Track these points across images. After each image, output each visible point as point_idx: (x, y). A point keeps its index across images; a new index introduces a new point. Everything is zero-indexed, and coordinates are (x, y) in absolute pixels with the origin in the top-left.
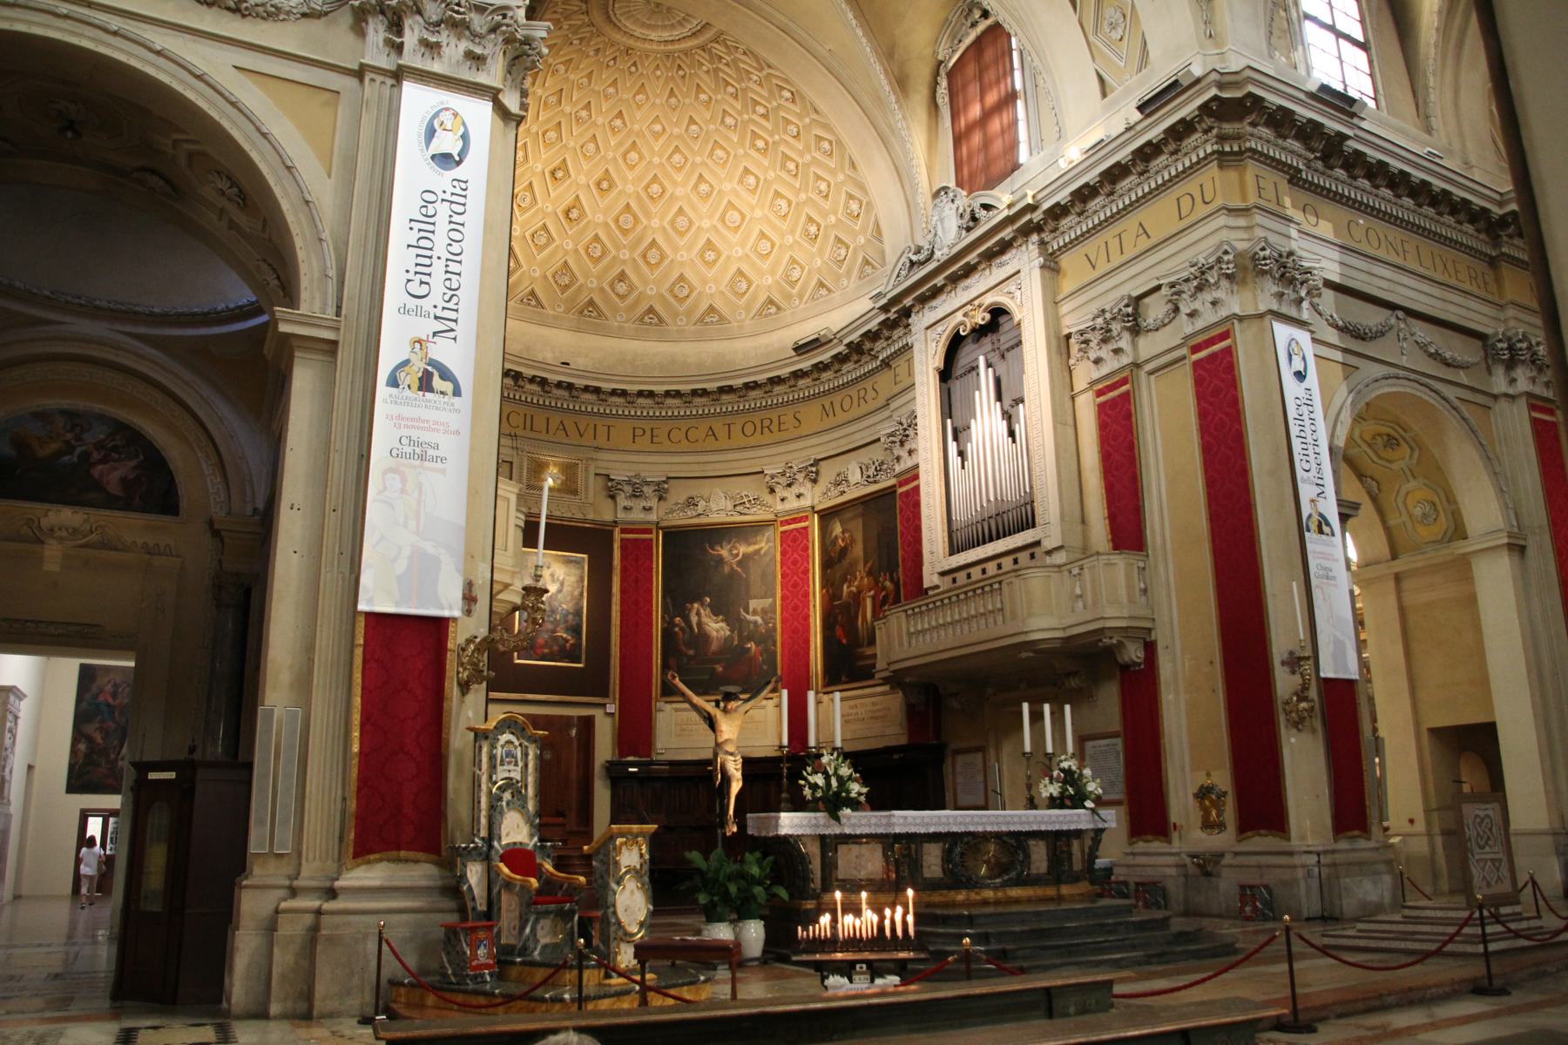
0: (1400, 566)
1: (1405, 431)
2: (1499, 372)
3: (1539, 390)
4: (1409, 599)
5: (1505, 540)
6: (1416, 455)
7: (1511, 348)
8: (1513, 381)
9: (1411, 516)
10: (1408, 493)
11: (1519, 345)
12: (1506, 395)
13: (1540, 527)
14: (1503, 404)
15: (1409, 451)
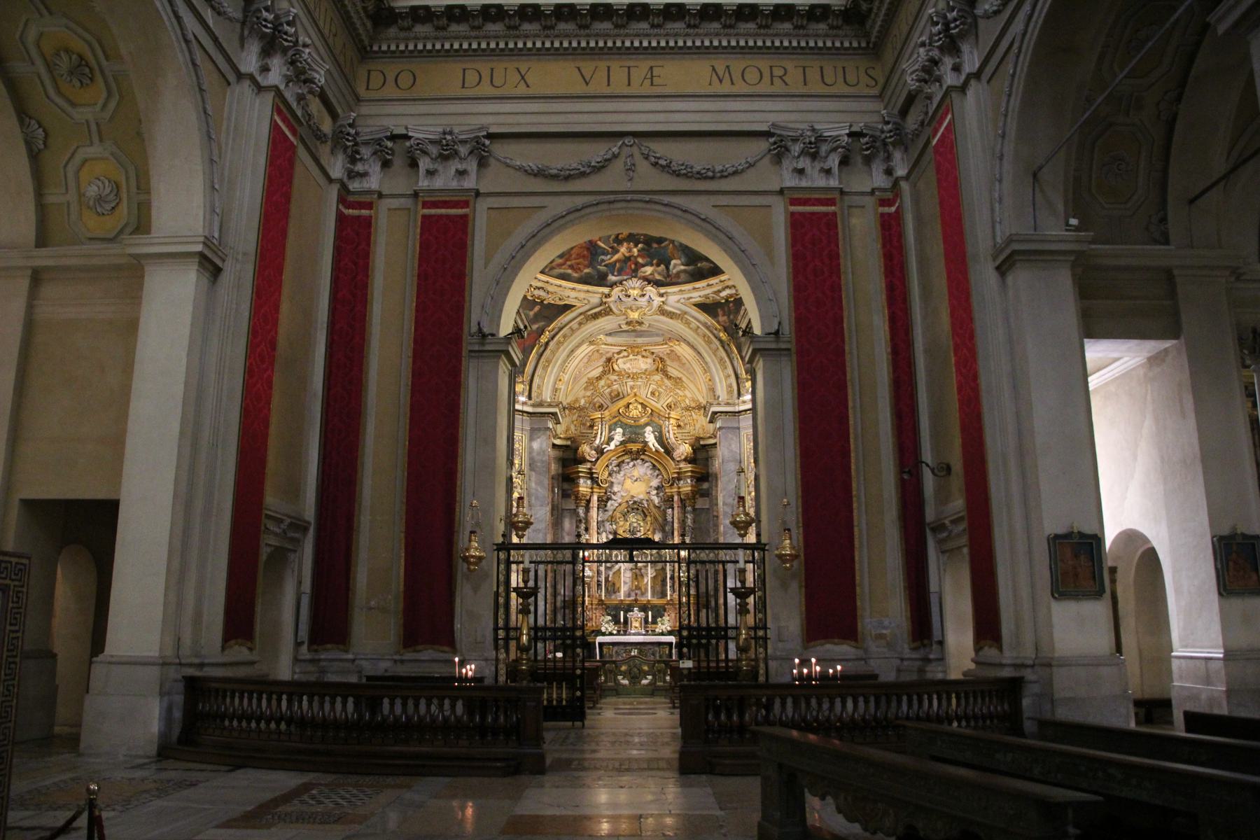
0: (44, 258)
1: (107, 58)
2: (254, 48)
3: (289, 96)
4: (45, 311)
5: (199, 248)
6: (112, 105)
7: (277, 26)
8: (265, 69)
9: (81, 195)
10: (85, 161)
11: (286, 27)
12: (251, 77)
13: (245, 254)
14: (246, 87)
15: (104, 95)
